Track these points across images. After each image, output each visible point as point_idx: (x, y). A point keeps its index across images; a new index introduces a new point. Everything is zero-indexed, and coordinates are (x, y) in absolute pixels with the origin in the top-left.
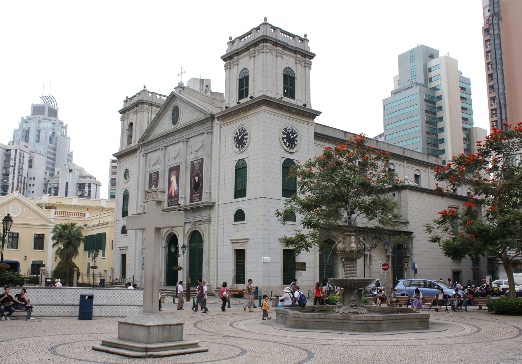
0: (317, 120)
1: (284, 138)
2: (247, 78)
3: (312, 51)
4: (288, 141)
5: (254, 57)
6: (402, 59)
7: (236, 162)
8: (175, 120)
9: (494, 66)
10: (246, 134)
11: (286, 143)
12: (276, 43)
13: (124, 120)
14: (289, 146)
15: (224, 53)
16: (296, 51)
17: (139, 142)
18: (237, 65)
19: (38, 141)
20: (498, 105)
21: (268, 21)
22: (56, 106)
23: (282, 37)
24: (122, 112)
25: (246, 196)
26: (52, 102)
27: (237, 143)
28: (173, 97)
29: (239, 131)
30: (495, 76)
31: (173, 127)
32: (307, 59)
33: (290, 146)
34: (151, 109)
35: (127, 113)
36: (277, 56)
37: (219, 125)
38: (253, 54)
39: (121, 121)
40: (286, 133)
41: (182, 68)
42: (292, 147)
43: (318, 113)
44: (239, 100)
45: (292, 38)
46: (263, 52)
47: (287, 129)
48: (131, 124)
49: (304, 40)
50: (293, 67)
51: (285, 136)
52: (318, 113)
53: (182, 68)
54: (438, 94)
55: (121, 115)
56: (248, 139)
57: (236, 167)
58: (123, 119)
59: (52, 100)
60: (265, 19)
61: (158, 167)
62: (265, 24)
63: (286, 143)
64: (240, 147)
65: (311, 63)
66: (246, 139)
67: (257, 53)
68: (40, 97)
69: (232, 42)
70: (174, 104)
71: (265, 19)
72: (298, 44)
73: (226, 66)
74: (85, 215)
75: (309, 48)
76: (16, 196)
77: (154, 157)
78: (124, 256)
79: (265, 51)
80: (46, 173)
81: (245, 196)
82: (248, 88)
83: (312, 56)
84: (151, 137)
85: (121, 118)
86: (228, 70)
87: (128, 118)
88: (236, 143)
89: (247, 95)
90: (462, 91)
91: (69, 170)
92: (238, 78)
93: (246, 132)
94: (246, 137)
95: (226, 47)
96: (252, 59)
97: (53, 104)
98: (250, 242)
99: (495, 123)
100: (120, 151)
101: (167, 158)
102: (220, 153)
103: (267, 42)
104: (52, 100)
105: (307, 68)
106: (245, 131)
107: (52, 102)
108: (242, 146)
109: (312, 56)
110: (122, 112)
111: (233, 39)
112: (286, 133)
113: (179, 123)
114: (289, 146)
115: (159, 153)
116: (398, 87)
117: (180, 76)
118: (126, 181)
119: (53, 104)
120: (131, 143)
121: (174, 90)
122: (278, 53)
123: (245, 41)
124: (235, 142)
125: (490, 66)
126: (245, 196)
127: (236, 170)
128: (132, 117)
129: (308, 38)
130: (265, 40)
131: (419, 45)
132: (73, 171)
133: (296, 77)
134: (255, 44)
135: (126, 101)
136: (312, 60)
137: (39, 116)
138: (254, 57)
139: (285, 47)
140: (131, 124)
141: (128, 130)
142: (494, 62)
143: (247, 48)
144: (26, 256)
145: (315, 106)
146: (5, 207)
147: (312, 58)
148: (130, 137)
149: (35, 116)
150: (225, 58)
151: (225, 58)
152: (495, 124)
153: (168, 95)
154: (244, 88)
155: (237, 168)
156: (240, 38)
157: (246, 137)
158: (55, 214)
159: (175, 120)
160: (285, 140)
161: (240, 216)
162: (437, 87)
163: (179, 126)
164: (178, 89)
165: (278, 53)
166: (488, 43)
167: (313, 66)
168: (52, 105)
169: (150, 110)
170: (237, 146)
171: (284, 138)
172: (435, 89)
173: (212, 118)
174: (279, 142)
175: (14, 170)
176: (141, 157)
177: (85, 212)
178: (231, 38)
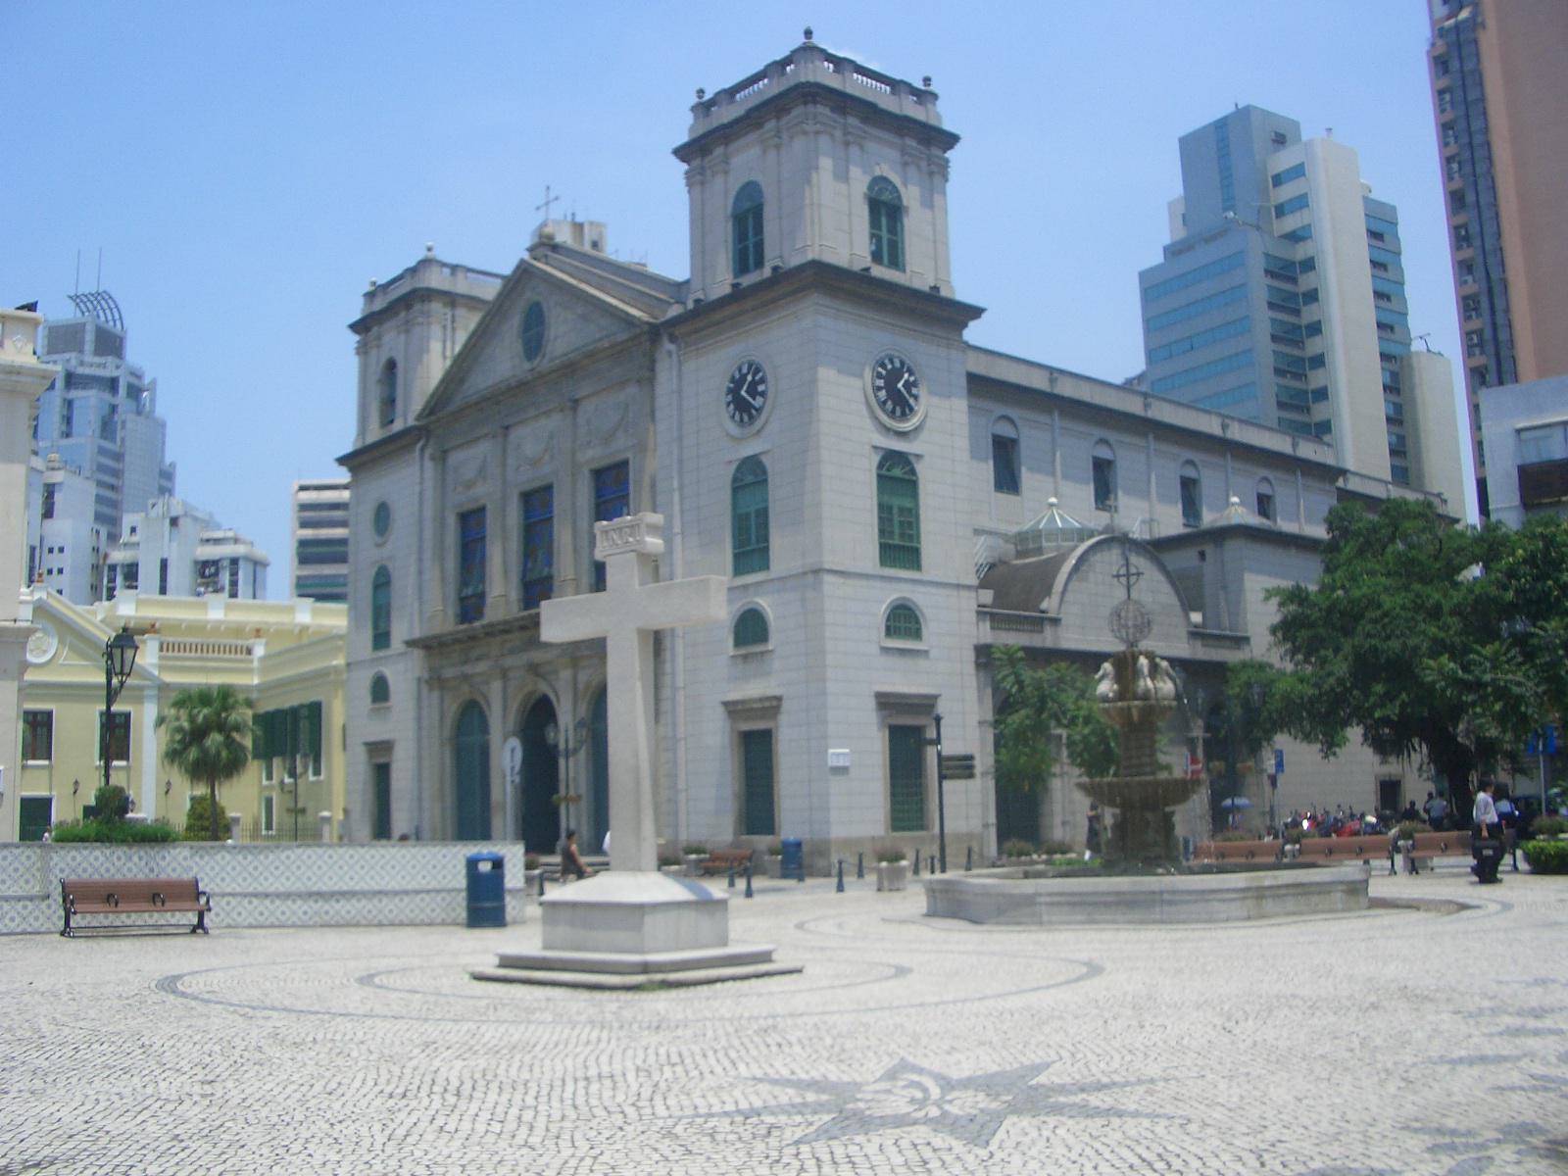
0: (974, 333)
1: (879, 389)
2: (757, 212)
3: (947, 126)
4: (889, 396)
5: (778, 147)
6: (1190, 146)
7: (734, 466)
8: (533, 344)
9: (1467, 169)
10: (763, 381)
11: (885, 402)
12: (843, 103)
14: (893, 412)
15: (683, 138)
16: (902, 126)
17: (419, 417)
18: (726, 172)
19: (68, 435)
20: (1484, 285)
21: (818, 41)
22: (118, 323)
23: (857, 85)
24: (359, 327)
25: (768, 568)
26: (108, 312)
27: (736, 409)
28: (523, 271)
29: (740, 370)
30: (1470, 198)
31: (527, 366)
32: (936, 151)
33: (898, 410)
34: (453, 316)
35: (375, 329)
36: (847, 144)
37: (675, 356)
38: (776, 139)
39: (358, 353)
40: (884, 372)
41: (548, 188)
42: (904, 414)
43: (976, 312)
44: (736, 276)
45: (888, 88)
46: (805, 133)
47: (887, 361)
48: (391, 366)
49: (924, 96)
50: (896, 179)
51: (881, 383)
52: (976, 312)
53: (548, 188)
54: (1300, 252)
55: (357, 338)
56: (770, 395)
57: (735, 480)
58: (363, 350)
59: (106, 306)
60: (808, 33)
61: (484, 492)
62: (808, 51)
63: (885, 402)
64: (746, 418)
65: (947, 161)
66: (763, 394)
67: (785, 136)
68: (71, 297)
69: (704, 108)
70: (529, 295)
71: (808, 33)
72: (910, 108)
73: (689, 175)
74: (249, 651)
75: (938, 117)
76: (40, 599)
77: (468, 459)
78: (382, 774)
79: (810, 127)
80: (98, 532)
81: (765, 565)
82: (762, 240)
83: (950, 140)
84: (458, 402)
86: (697, 189)
87: (379, 346)
88: (732, 407)
89: (759, 263)
90: (1375, 243)
91: (168, 521)
92: (730, 210)
93: (760, 374)
94: (761, 388)
95: (689, 119)
96: (772, 154)
97: (110, 318)
98: (786, 705)
99: (1475, 337)
100: (359, 445)
101: (511, 461)
102: (680, 439)
103: (815, 103)
104: (106, 306)
105: (937, 179)
106: (757, 370)
107: (108, 312)
108: (751, 417)
109: (950, 140)
110: (359, 327)
111: (707, 96)
112: (884, 372)
113: (547, 357)
114: (893, 412)
115: (484, 449)
116: (1181, 234)
117: (544, 209)
118: (379, 540)
119: (110, 318)
120: (392, 422)
121: (526, 256)
122: (849, 133)
123: (747, 99)
124: (728, 404)
125: (1455, 166)
126: (765, 565)
127: (735, 490)
128: (391, 340)
129: (933, 88)
130: (811, 93)
131: (1240, 107)
132: (181, 522)
133: (905, 203)
134: (775, 107)
135: (370, 296)
136: (949, 154)
137: (67, 356)
138: (778, 147)
139: (871, 113)
140: (391, 366)
141: (379, 381)
142: (1466, 155)
143: (753, 119)
145: (962, 290)
147: (951, 146)
148: (389, 403)
150: (682, 153)
151: (682, 153)
152: (1475, 341)
153: (507, 269)
154: (751, 243)
155: (737, 485)
156: (731, 93)
157: (761, 388)
158: (161, 650)
159: (533, 344)
160: (883, 394)
161: (750, 629)
162: (1299, 233)
163: (543, 364)
164: (540, 252)
165: (849, 133)
166: (1447, 97)
167: (953, 171)
168: (107, 321)
169: (449, 316)
170: (733, 417)
171: (879, 389)
172: (1295, 237)
173: (655, 333)
174: (863, 400)
176: (428, 464)
178: (701, 92)
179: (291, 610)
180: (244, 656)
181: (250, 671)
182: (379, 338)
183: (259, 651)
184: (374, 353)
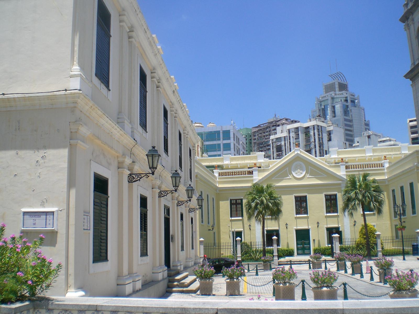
13: (409, 29)
19: (335, 117)
22: (345, 80)
26: (341, 78)
39: (406, 30)
58: (408, 27)
59: (340, 76)
68: (330, 76)
74: (382, 166)
80: (346, 143)
85: (404, 27)
87: (414, 24)
97: (342, 80)
100: (413, 67)
104: (340, 76)
107: (341, 78)
110: (405, 19)
119: (342, 80)
132: (371, 137)
137: (331, 93)
144: (318, 223)
146: (287, 168)
149: (328, 94)
168: (342, 81)
175: (315, 145)
177: (383, 161)
179: (399, 149)
180: (381, 168)
181: (383, 174)
182: (413, 20)
183: (387, 165)
184: (412, 27)
